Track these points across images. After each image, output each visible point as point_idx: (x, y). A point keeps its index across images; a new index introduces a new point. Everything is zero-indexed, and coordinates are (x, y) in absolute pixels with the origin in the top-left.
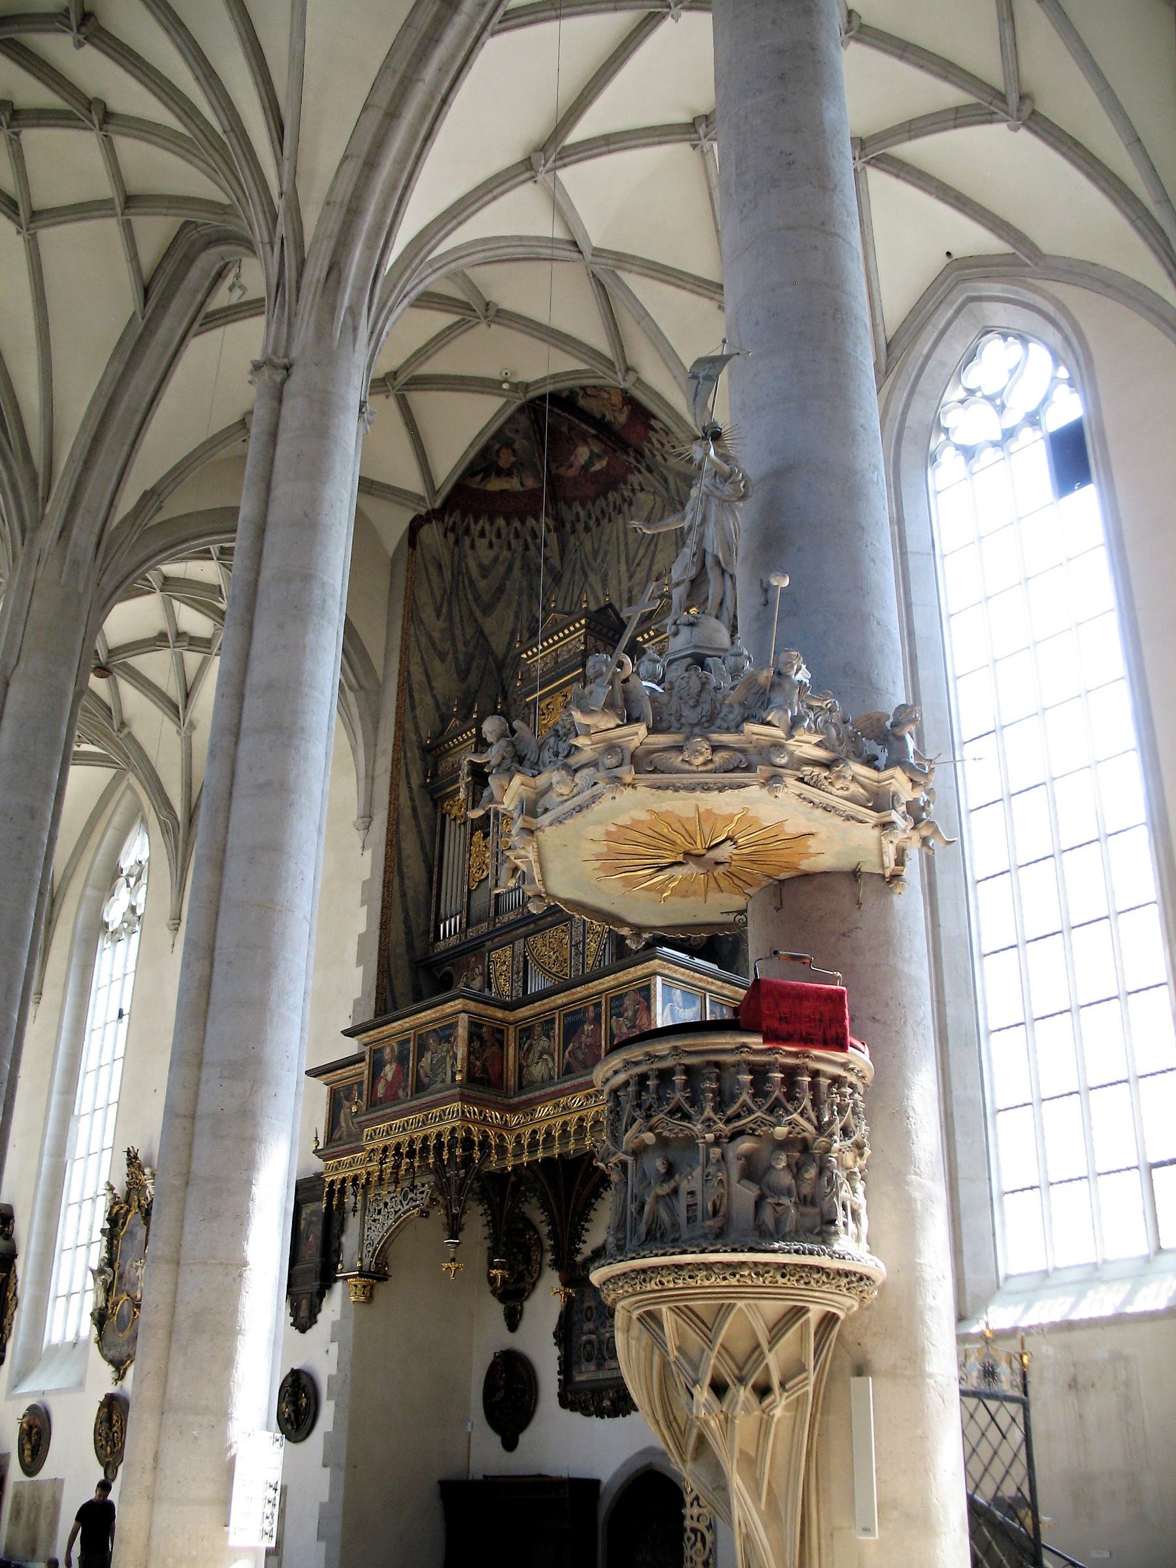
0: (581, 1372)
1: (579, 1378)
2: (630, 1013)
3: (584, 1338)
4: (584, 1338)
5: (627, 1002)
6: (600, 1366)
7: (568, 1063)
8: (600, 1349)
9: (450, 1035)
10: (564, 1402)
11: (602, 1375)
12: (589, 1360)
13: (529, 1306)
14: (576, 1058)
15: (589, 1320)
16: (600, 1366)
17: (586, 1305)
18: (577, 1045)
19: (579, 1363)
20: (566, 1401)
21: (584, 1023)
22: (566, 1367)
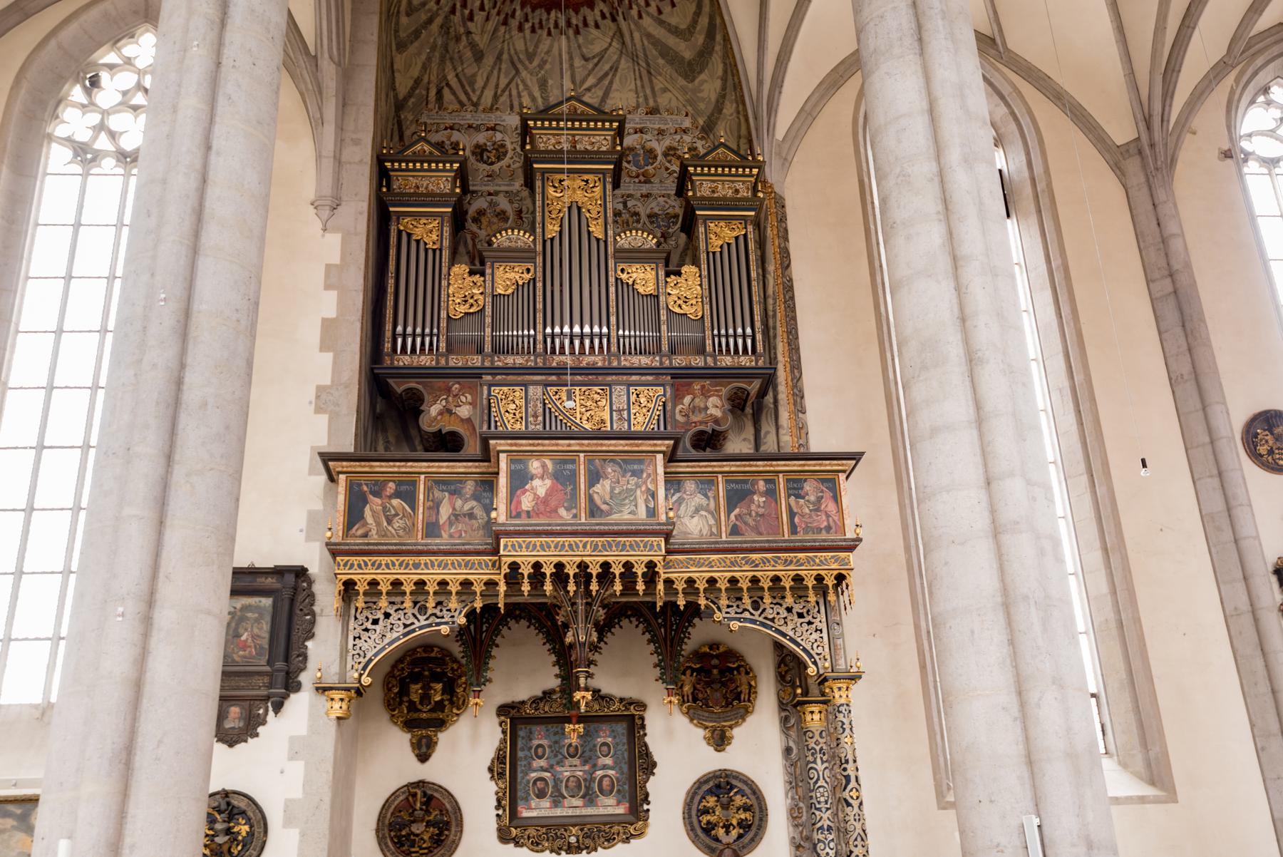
0: (530, 808)
1: (526, 814)
2: (812, 498)
3: (534, 775)
4: (534, 775)
5: (808, 487)
6: (556, 804)
7: (735, 526)
8: (556, 787)
9: (642, 471)
10: (504, 836)
11: (558, 812)
12: (541, 795)
13: (443, 738)
14: (746, 523)
15: (540, 758)
16: (556, 804)
17: (536, 742)
18: (745, 511)
19: (527, 799)
20: (504, 836)
21: (754, 493)
22: (509, 802)
